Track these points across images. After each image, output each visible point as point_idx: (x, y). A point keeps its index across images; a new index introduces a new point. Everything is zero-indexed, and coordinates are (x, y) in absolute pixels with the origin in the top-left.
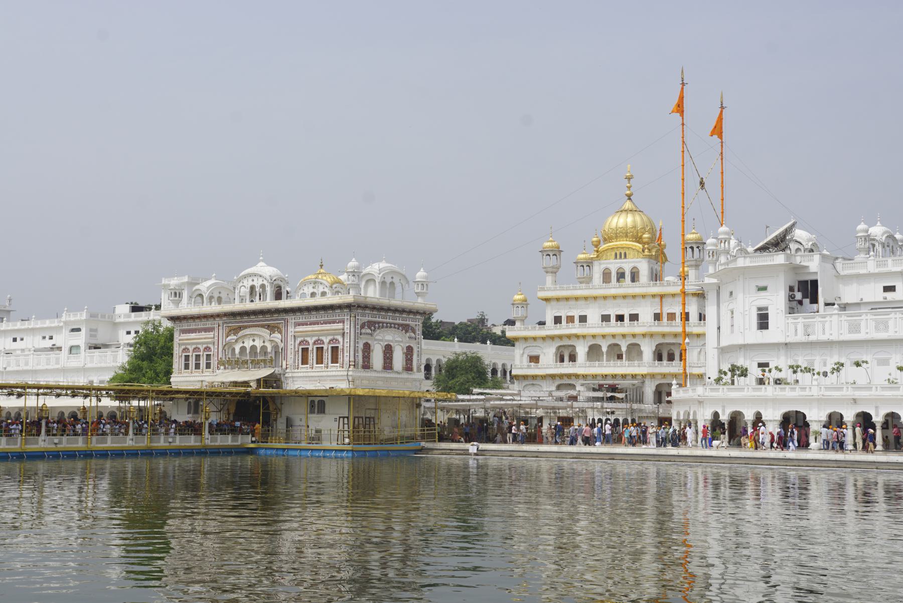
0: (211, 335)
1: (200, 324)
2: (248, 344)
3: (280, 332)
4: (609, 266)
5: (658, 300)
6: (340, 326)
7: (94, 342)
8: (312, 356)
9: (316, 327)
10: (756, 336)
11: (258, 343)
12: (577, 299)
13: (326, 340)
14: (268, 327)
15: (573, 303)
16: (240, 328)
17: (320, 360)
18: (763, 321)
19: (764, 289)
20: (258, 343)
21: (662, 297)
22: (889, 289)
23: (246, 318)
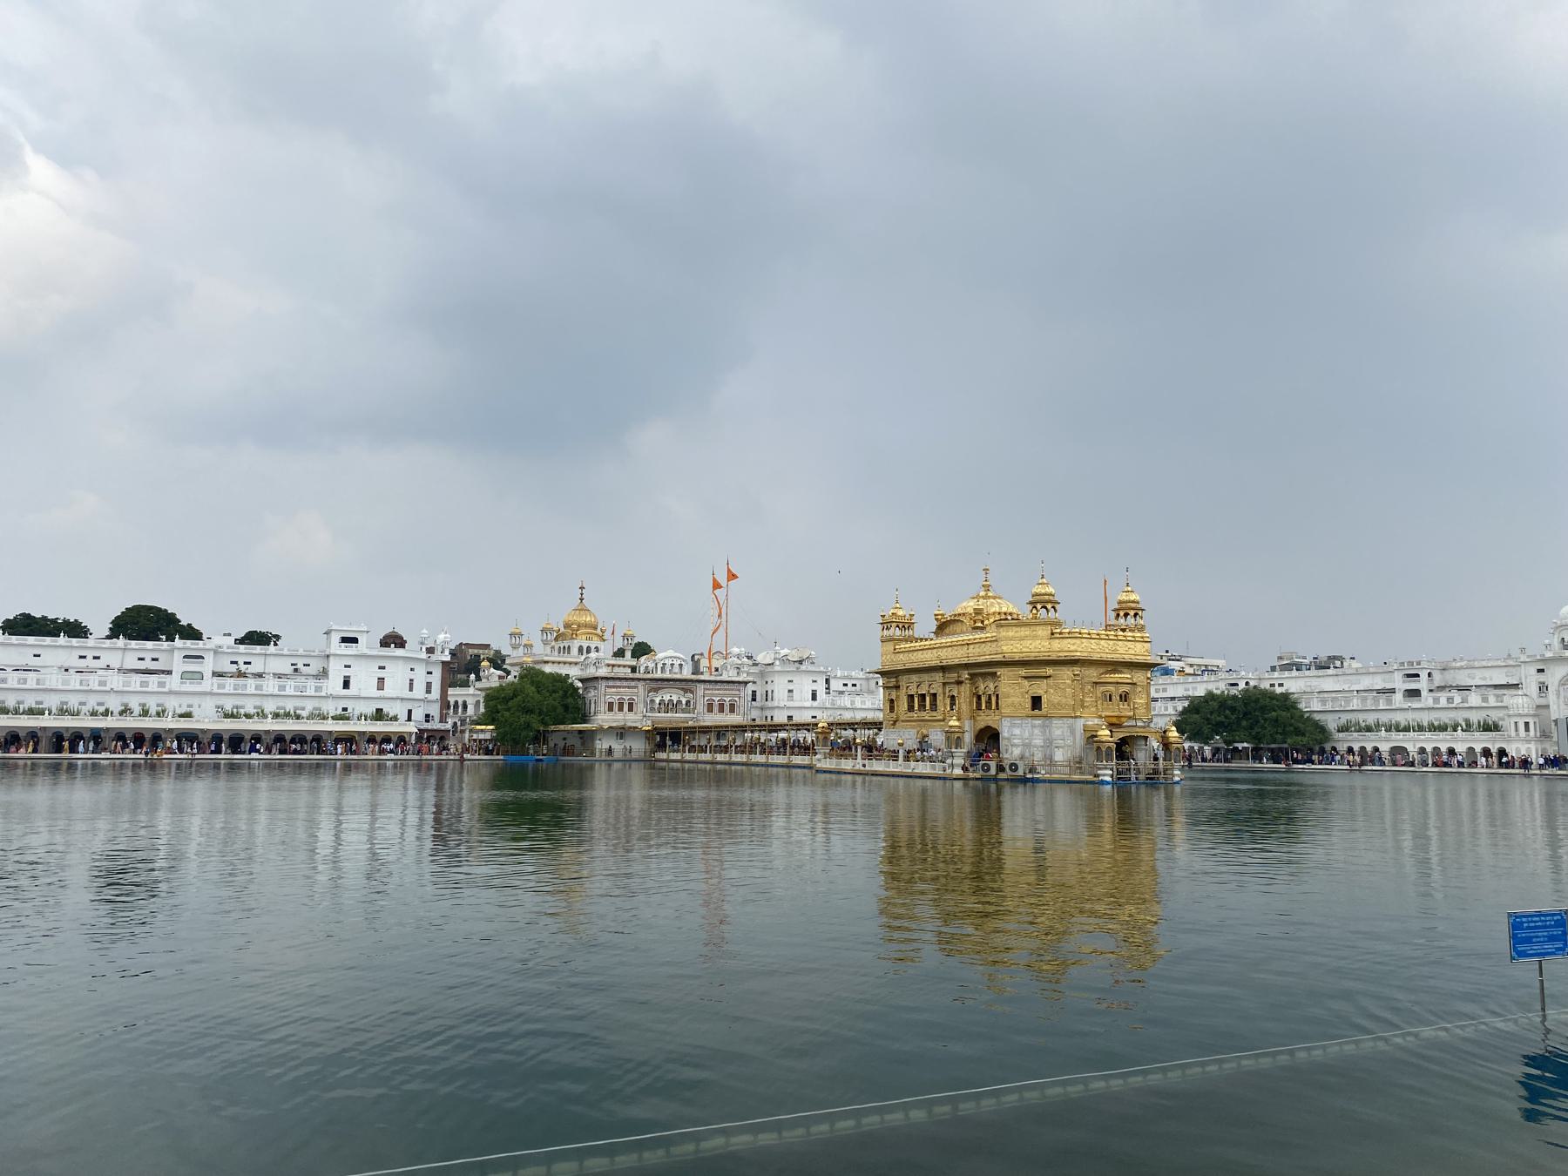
0: (636, 691)
1: (625, 684)
2: (667, 698)
3: (692, 692)
4: (582, 644)
5: (610, 668)
6: (737, 693)
7: (218, 669)
8: (716, 709)
9: (721, 692)
10: (809, 703)
11: (675, 699)
12: (565, 663)
13: (727, 699)
14: (682, 689)
15: (561, 665)
16: (660, 688)
17: (721, 709)
18: (814, 697)
19: (816, 681)
20: (675, 699)
21: (613, 666)
22: (845, 685)
23: (666, 683)
